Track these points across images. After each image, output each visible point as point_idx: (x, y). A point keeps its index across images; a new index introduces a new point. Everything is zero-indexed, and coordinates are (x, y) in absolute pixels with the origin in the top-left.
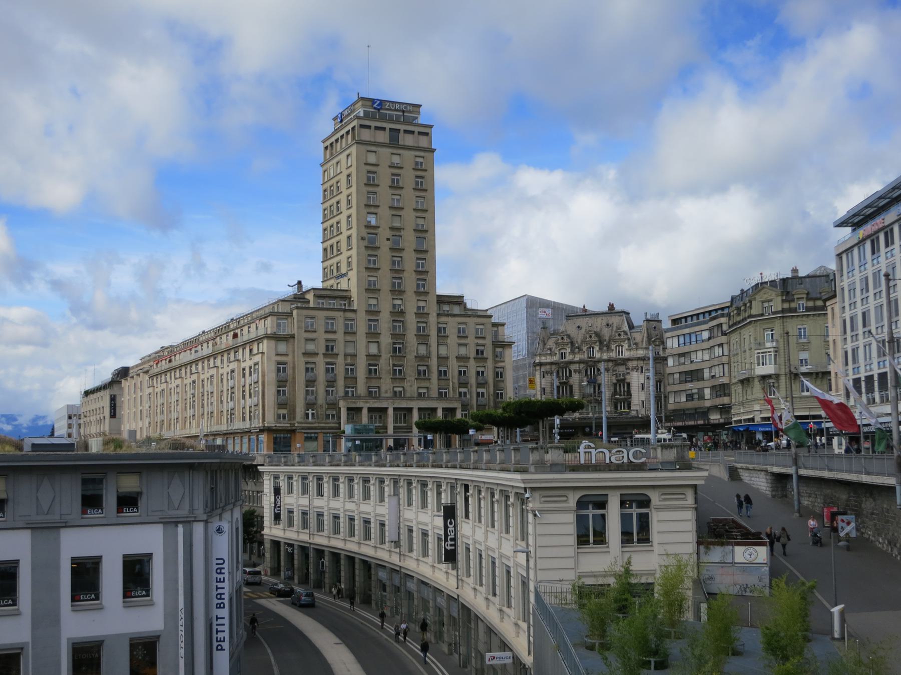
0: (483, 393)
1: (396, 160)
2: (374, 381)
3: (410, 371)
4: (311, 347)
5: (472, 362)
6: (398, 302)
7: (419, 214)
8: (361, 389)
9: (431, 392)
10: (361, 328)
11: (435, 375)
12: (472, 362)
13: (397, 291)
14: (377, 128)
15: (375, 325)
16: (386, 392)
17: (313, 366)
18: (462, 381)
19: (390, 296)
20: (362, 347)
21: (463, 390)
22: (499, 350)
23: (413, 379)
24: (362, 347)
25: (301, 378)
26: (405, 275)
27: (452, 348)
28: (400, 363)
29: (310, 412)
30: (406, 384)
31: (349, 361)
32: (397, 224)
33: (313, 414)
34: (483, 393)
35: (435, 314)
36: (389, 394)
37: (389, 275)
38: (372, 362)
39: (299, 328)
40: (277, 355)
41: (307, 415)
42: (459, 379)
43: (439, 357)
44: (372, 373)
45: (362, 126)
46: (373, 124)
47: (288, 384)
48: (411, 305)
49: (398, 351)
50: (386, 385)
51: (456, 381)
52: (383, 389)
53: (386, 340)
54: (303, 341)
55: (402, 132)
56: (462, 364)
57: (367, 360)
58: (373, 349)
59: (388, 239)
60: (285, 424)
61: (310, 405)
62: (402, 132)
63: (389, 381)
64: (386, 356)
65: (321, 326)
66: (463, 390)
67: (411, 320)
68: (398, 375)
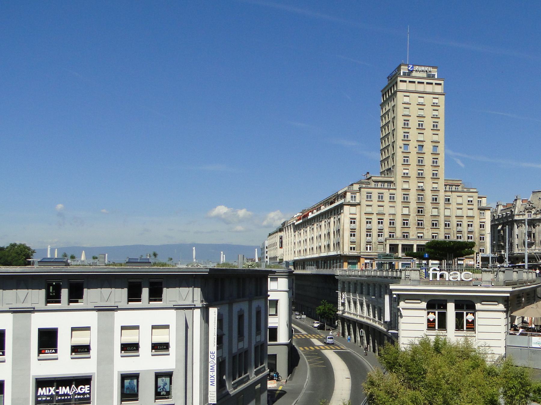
0: (471, 237)
1: (421, 100)
3: (427, 223)
4: (369, 210)
6: (421, 184)
8: (399, 234)
9: (440, 236)
10: (399, 198)
11: (442, 226)
13: (420, 177)
15: (407, 197)
16: (413, 235)
17: (370, 220)
18: (458, 230)
19: (416, 180)
20: (399, 210)
21: (459, 235)
22: (482, 212)
23: (429, 228)
24: (399, 210)
25: (364, 226)
26: (425, 168)
27: (453, 212)
28: (422, 219)
29: (369, 246)
30: (425, 231)
31: (391, 218)
32: (421, 138)
33: (370, 247)
34: (471, 237)
35: (443, 191)
36: (415, 237)
37: (416, 168)
38: (405, 219)
41: (367, 248)
42: (457, 229)
44: (405, 223)
45: (401, 81)
46: (408, 80)
48: (428, 185)
49: (420, 211)
50: (413, 232)
51: (455, 229)
52: (411, 234)
53: (413, 205)
54: (365, 206)
56: (459, 220)
58: (406, 211)
59: (416, 147)
61: (369, 243)
63: (415, 229)
65: (375, 197)
66: (459, 235)
67: (428, 196)
68: (420, 224)
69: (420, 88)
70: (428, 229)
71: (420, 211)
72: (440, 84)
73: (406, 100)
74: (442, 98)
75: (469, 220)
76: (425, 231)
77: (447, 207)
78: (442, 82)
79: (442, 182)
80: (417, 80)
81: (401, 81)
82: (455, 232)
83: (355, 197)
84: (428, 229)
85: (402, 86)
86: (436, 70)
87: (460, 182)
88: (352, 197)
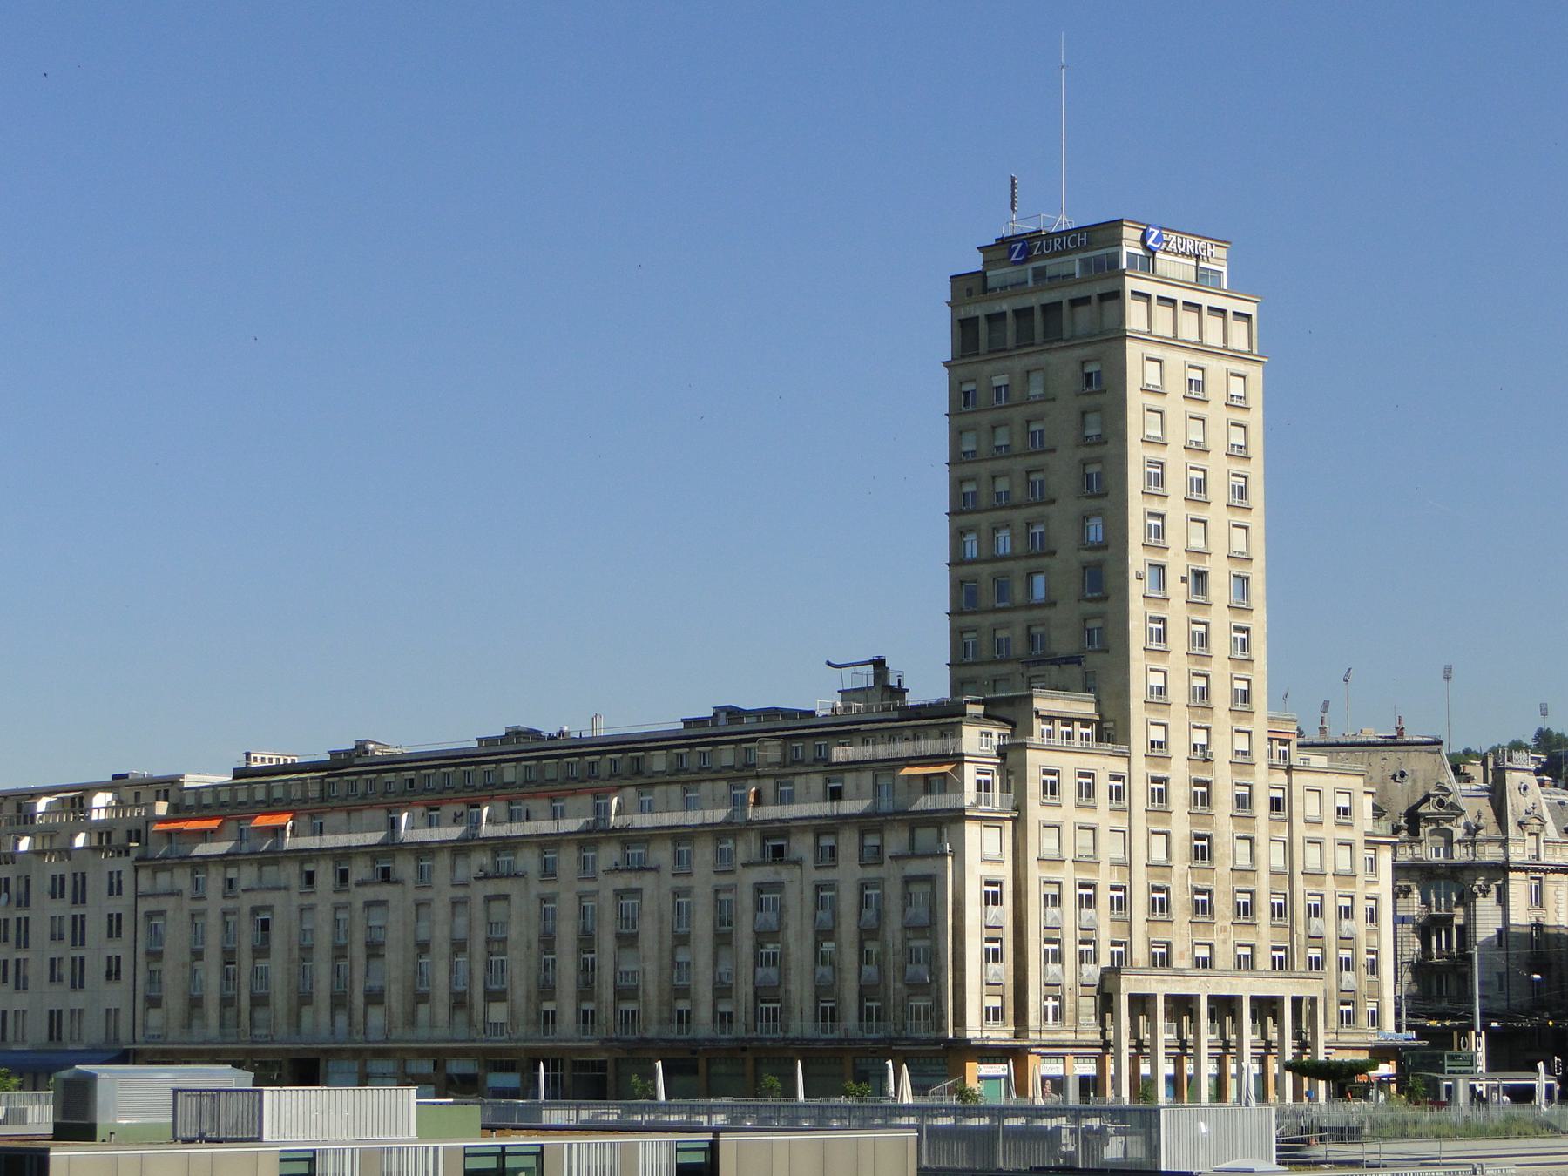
2: (1160, 926)
3: (1223, 907)
23: (1228, 924)
32: (1197, 543)
33: (1055, 1008)
40: (984, 861)
49: (1203, 852)
53: (1181, 826)
57: (1149, 876)
60: (1001, 1034)
64: (1181, 863)
68: (1203, 908)
70: (1224, 929)
71: (1203, 852)
72: (1248, 317)
74: (1255, 372)
76: (1216, 938)
78: (1250, 308)
79: (1260, 726)
82: (1303, 942)
84: (1224, 929)
85: (1135, 316)
86: (1222, 253)
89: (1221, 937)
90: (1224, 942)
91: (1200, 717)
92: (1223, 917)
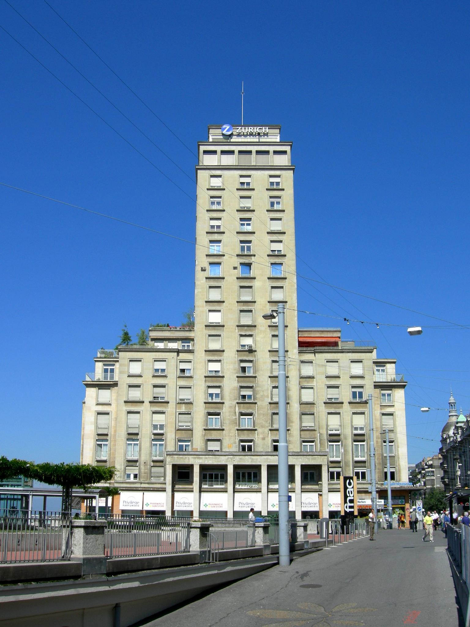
4: (135, 394)
5: (346, 406)
7: (275, 237)
12: (346, 406)
14: (223, 152)
16: (229, 447)
23: (266, 430)
39: (121, 372)
40: (98, 404)
43: (301, 404)
45: (205, 152)
47: (108, 438)
48: (262, 341)
55: (254, 153)
59: (235, 268)
62: (254, 153)
69: (245, 160)
72: (285, 152)
73: (216, 182)
75: (355, 410)
77: (305, 384)
80: (236, 149)
81: (205, 152)
82: (325, 437)
83: (112, 371)
87: (338, 335)
88: (106, 371)
89: (261, 436)
90: (263, 439)
91: (246, 330)
92: (262, 427)
